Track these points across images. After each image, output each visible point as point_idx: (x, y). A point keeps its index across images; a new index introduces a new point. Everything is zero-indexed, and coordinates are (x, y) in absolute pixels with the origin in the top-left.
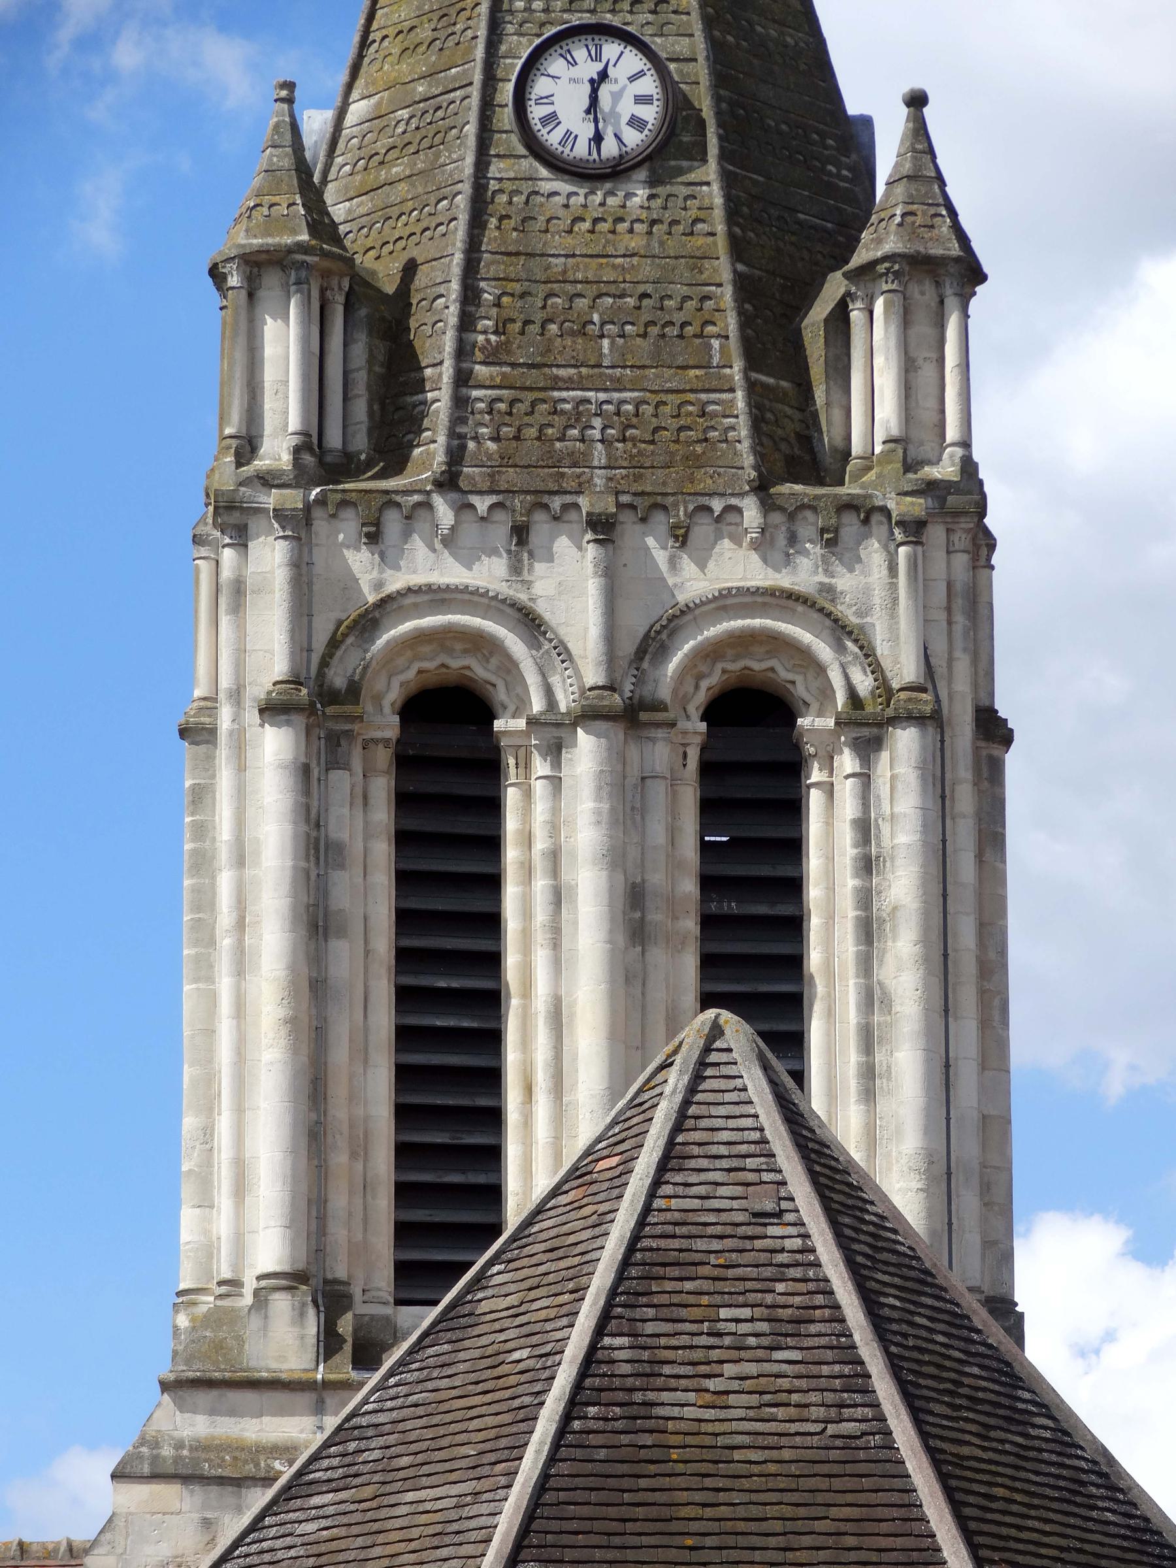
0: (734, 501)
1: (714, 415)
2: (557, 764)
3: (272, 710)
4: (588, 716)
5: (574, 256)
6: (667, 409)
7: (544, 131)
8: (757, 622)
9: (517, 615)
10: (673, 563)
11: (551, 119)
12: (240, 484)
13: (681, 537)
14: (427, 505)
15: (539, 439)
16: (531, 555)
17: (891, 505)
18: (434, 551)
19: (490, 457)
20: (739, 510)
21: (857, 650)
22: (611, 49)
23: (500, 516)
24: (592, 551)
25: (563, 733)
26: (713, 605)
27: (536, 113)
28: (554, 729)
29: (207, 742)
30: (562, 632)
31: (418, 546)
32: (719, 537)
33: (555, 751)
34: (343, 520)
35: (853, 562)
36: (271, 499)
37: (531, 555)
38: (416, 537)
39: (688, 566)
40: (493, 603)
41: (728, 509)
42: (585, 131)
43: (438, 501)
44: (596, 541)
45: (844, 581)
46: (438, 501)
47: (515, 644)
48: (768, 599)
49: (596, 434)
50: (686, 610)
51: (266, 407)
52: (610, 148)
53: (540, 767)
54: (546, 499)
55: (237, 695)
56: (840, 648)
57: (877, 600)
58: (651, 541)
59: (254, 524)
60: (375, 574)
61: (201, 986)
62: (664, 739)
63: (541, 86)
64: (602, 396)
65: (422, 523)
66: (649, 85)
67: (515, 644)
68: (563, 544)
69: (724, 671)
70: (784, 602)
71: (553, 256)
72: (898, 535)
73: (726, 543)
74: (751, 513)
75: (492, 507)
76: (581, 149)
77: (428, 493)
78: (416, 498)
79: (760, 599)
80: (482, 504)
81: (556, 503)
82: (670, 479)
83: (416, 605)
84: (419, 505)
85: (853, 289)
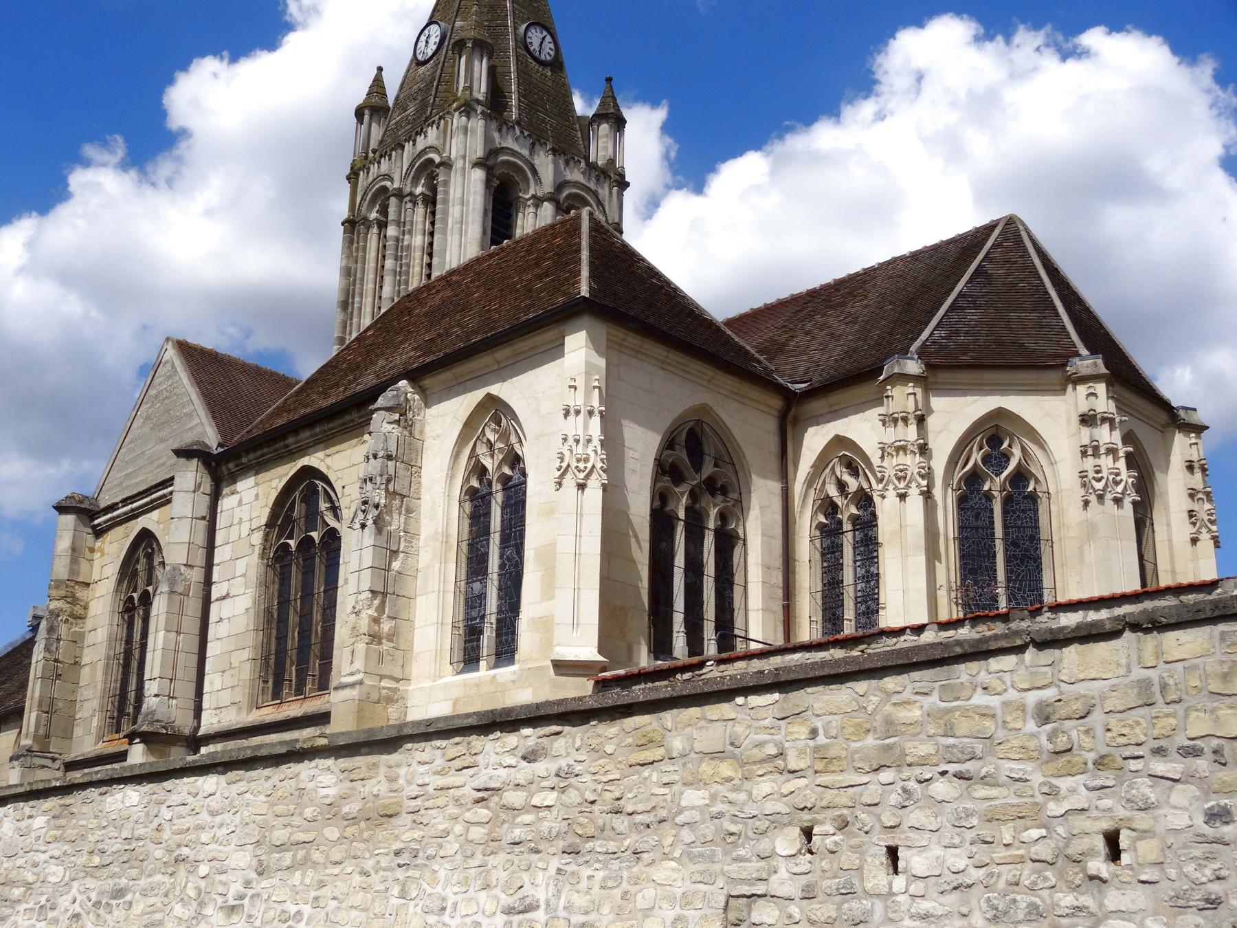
3: (478, 164)
11: (531, 43)
13: (567, 163)
14: (514, 128)
22: (545, 33)
24: (551, 157)
27: (528, 40)
31: (509, 137)
33: (537, 206)
35: (603, 188)
36: (479, 109)
39: (568, 172)
45: (600, 191)
47: (530, 176)
52: (543, 57)
53: (532, 209)
55: (464, 157)
59: (473, 114)
63: (529, 34)
65: (511, 131)
66: (552, 46)
67: (530, 176)
74: (583, 164)
76: (537, 54)
80: (526, 133)
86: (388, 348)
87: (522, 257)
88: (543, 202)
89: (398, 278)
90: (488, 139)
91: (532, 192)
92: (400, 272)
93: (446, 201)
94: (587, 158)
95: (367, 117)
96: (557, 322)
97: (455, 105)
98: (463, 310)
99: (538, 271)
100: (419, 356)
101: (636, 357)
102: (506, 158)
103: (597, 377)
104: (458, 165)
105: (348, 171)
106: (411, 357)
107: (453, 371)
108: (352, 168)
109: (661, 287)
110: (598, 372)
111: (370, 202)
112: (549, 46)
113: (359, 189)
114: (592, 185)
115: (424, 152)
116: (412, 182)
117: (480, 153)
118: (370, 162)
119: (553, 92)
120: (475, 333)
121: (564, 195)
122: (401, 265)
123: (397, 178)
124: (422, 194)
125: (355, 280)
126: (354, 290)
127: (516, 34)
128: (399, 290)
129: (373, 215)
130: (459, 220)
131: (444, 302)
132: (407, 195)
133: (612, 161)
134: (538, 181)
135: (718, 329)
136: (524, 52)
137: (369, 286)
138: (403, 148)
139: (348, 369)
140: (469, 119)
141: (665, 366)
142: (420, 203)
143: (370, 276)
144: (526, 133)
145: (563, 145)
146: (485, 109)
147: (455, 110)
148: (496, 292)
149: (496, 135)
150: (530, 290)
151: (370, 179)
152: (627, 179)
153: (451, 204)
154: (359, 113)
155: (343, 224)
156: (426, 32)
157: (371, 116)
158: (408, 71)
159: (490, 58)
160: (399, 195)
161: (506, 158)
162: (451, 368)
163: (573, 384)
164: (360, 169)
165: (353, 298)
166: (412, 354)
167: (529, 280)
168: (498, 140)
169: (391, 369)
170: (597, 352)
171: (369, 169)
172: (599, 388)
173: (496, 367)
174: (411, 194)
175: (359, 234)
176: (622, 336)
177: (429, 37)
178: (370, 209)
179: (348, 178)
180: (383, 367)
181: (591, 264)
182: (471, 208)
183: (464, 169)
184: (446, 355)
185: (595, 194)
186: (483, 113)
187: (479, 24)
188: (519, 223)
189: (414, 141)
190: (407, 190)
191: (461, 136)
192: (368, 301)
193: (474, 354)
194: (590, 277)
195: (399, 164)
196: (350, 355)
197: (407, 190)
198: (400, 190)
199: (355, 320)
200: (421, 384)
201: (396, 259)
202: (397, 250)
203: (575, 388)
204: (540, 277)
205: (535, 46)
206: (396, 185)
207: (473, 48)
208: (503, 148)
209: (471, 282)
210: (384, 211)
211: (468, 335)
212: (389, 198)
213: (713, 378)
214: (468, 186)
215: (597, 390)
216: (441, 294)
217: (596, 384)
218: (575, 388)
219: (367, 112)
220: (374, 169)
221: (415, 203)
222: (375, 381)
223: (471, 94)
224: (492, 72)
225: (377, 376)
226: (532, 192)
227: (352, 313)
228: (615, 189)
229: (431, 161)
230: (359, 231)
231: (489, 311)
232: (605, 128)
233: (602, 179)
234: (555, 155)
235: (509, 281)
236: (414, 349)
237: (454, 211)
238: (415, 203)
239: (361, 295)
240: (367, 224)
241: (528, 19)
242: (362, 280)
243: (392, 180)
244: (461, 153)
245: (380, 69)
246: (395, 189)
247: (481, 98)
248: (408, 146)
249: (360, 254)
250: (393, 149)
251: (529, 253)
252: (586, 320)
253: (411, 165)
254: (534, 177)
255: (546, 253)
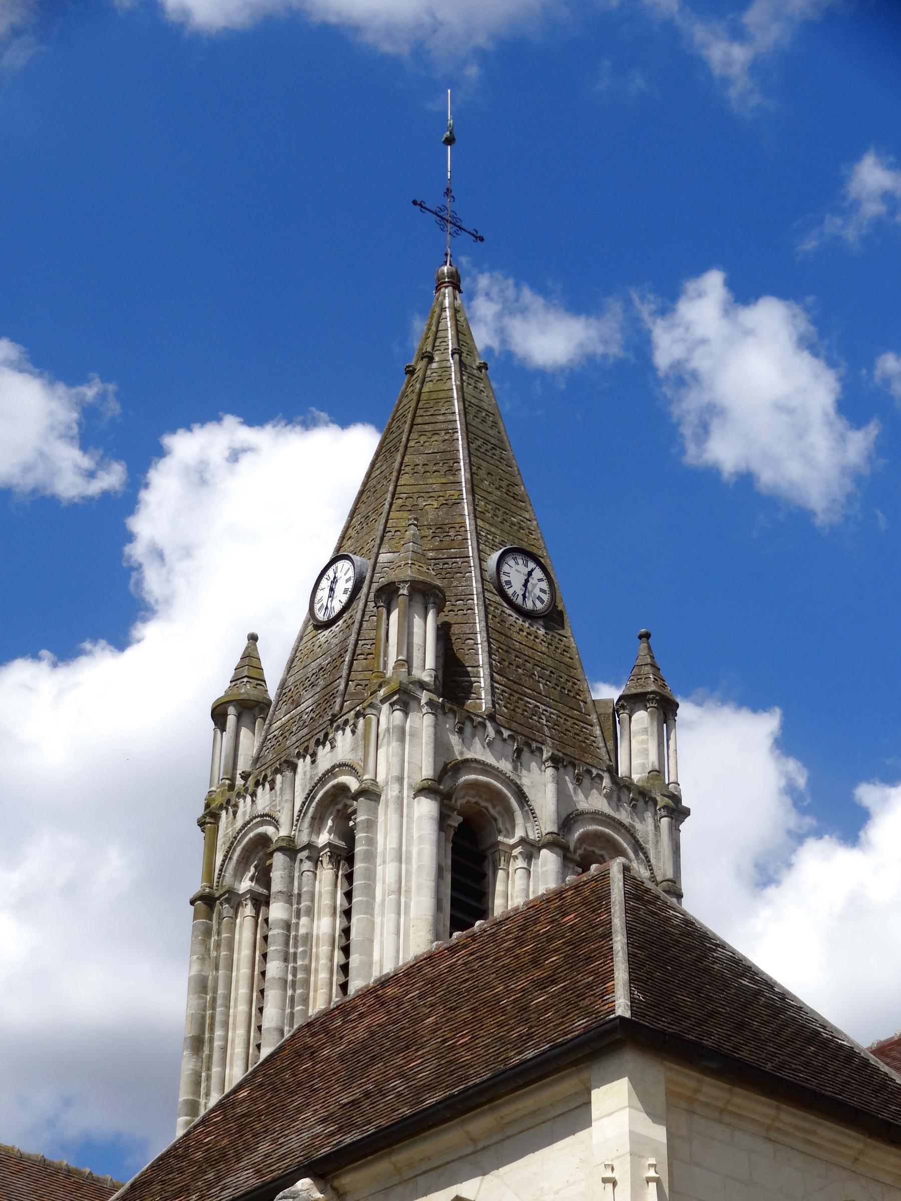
0: (601, 772)
1: (586, 734)
2: (529, 864)
3: (423, 791)
4: (551, 845)
5: (522, 644)
6: (569, 723)
7: (506, 587)
8: (607, 830)
9: (516, 790)
10: (575, 789)
11: (508, 583)
12: (411, 683)
13: (578, 780)
14: (485, 726)
15: (522, 714)
16: (521, 765)
17: (658, 799)
18: (484, 748)
19: (505, 713)
20: (601, 778)
21: (644, 858)
22: (531, 565)
23: (510, 742)
24: (550, 772)
25: (535, 851)
26: (590, 816)
27: (504, 578)
28: (529, 847)
29: (375, 801)
30: (533, 804)
32: (592, 789)
33: (529, 857)
34: (448, 717)
35: (642, 820)
36: (424, 697)
37: (521, 765)
38: (477, 738)
39: (581, 796)
40: (507, 780)
41: (598, 775)
42: (520, 593)
43: (488, 724)
44: (553, 767)
45: (638, 826)
46: (488, 724)
48: (612, 822)
49: (544, 722)
50: (582, 813)
51: (414, 654)
52: (529, 605)
53: (520, 863)
54: (530, 741)
55: (400, 780)
56: (637, 855)
57: (650, 839)
58: (567, 778)
59: (413, 704)
60: (460, 747)
61: (369, 916)
62: (572, 868)
63: (505, 568)
64: (544, 707)
65: (480, 731)
66: (544, 585)
68: (534, 765)
69: (585, 850)
70: (617, 825)
71: (515, 640)
72: (663, 813)
73: (595, 791)
74: (606, 782)
75: (509, 736)
76: (520, 601)
77: (485, 719)
78: (480, 719)
79: (608, 820)
80: (506, 733)
81: (534, 745)
82: (577, 753)
83: (476, 768)
84: (480, 722)
85: (625, 704)
86: (275, 1120)
87: (508, 950)
88: (540, 849)
89: (290, 992)
90: (440, 746)
91: (519, 833)
92: (294, 983)
93: (370, 856)
94: (613, 771)
95: (231, 720)
96: (576, 1063)
97: (382, 693)
98: (407, 1047)
99: (537, 974)
100: (332, 1134)
101: (721, 1122)
102: (472, 777)
103: (652, 1161)
104: (390, 793)
105: (200, 811)
106: (318, 1136)
107: (394, 1159)
108: (207, 806)
109: (758, 993)
110: (655, 1154)
111: (239, 862)
112: (538, 584)
113: (220, 842)
114: (623, 816)
115: (331, 773)
116: (311, 825)
117: (427, 770)
118: (239, 795)
119: (550, 662)
120: (430, 1088)
121: (577, 835)
122: (295, 970)
123: (284, 818)
124: (329, 845)
125: (214, 1000)
126: (213, 1017)
127: (482, 570)
128: (292, 1015)
129: (245, 885)
130: (394, 887)
131: (373, 1034)
132: (303, 849)
133: (657, 773)
134: (531, 813)
135: (865, 1063)
136: (498, 599)
137: (240, 1009)
138: (294, 768)
139: (206, 1160)
140: (406, 714)
141: (773, 1135)
142: (325, 860)
143: (241, 991)
144: (506, 733)
145: (569, 751)
146: (435, 697)
147: (383, 701)
148: (464, 1013)
149: (454, 739)
150: (525, 1009)
151: (239, 823)
152: (685, 803)
153: (379, 861)
154: (218, 715)
155: (192, 903)
156: (330, 573)
157: (239, 717)
158: (301, 638)
159: (439, 611)
160: (290, 849)
161: (472, 777)
162: (390, 1154)
163: (609, 1174)
164: (221, 807)
165: (212, 1030)
166: (319, 1129)
167: (523, 990)
168: (458, 749)
169: (282, 1158)
170: (649, 1114)
171: (236, 806)
172: (657, 1181)
173: (470, 1150)
174: (309, 846)
175: (220, 919)
176: (692, 1084)
177: (335, 581)
178: (239, 874)
179: (201, 824)
180: (267, 1156)
181: (632, 958)
182: (414, 866)
183: (400, 799)
184: (380, 1131)
185: (629, 832)
186: (430, 703)
187: (419, 557)
188: (499, 887)
189: (314, 755)
190: (303, 839)
191: (395, 744)
192: (238, 1035)
193: (430, 1127)
194: (631, 981)
195: (288, 796)
196: (208, 1134)
197: (303, 839)
198: (290, 839)
199: (216, 1069)
200: (336, 1183)
201: (286, 960)
202: (287, 944)
203: (614, 1183)
204: (541, 985)
205: (515, 588)
206: (284, 832)
207: (410, 596)
208: (466, 761)
209: (420, 997)
210: (264, 877)
211: (419, 1092)
212: (271, 855)
213: (862, 1152)
214: (409, 828)
215: (653, 1186)
216: (367, 1021)
217: (652, 1173)
218: (614, 1183)
219: (231, 710)
220: (245, 807)
221: (316, 861)
222: (255, 1182)
223: (409, 673)
224: (444, 633)
225: (258, 1171)
226: (519, 833)
227: (210, 1057)
228: (665, 821)
229: (343, 789)
230: (220, 914)
231: (452, 1048)
232: (642, 718)
233: (641, 804)
234: (556, 768)
235: (488, 994)
236: (323, 1120)
237: (386, 873)
238: (316, 861)
239: (226, 1025)
240: (234, 899)
241: (503, 543)
242: (227, 998)
243: (275, 823)
244: (395, 772)
245: (253, 638)
246: (282, 839)
247: (426, 677)
248: (303, 765)
249: (224, 953)
250: (277, 771)
251: (520, 941)
252: (629, 1058)
253: (310, 796)
254: (522, 807)
255: (550, 940)
